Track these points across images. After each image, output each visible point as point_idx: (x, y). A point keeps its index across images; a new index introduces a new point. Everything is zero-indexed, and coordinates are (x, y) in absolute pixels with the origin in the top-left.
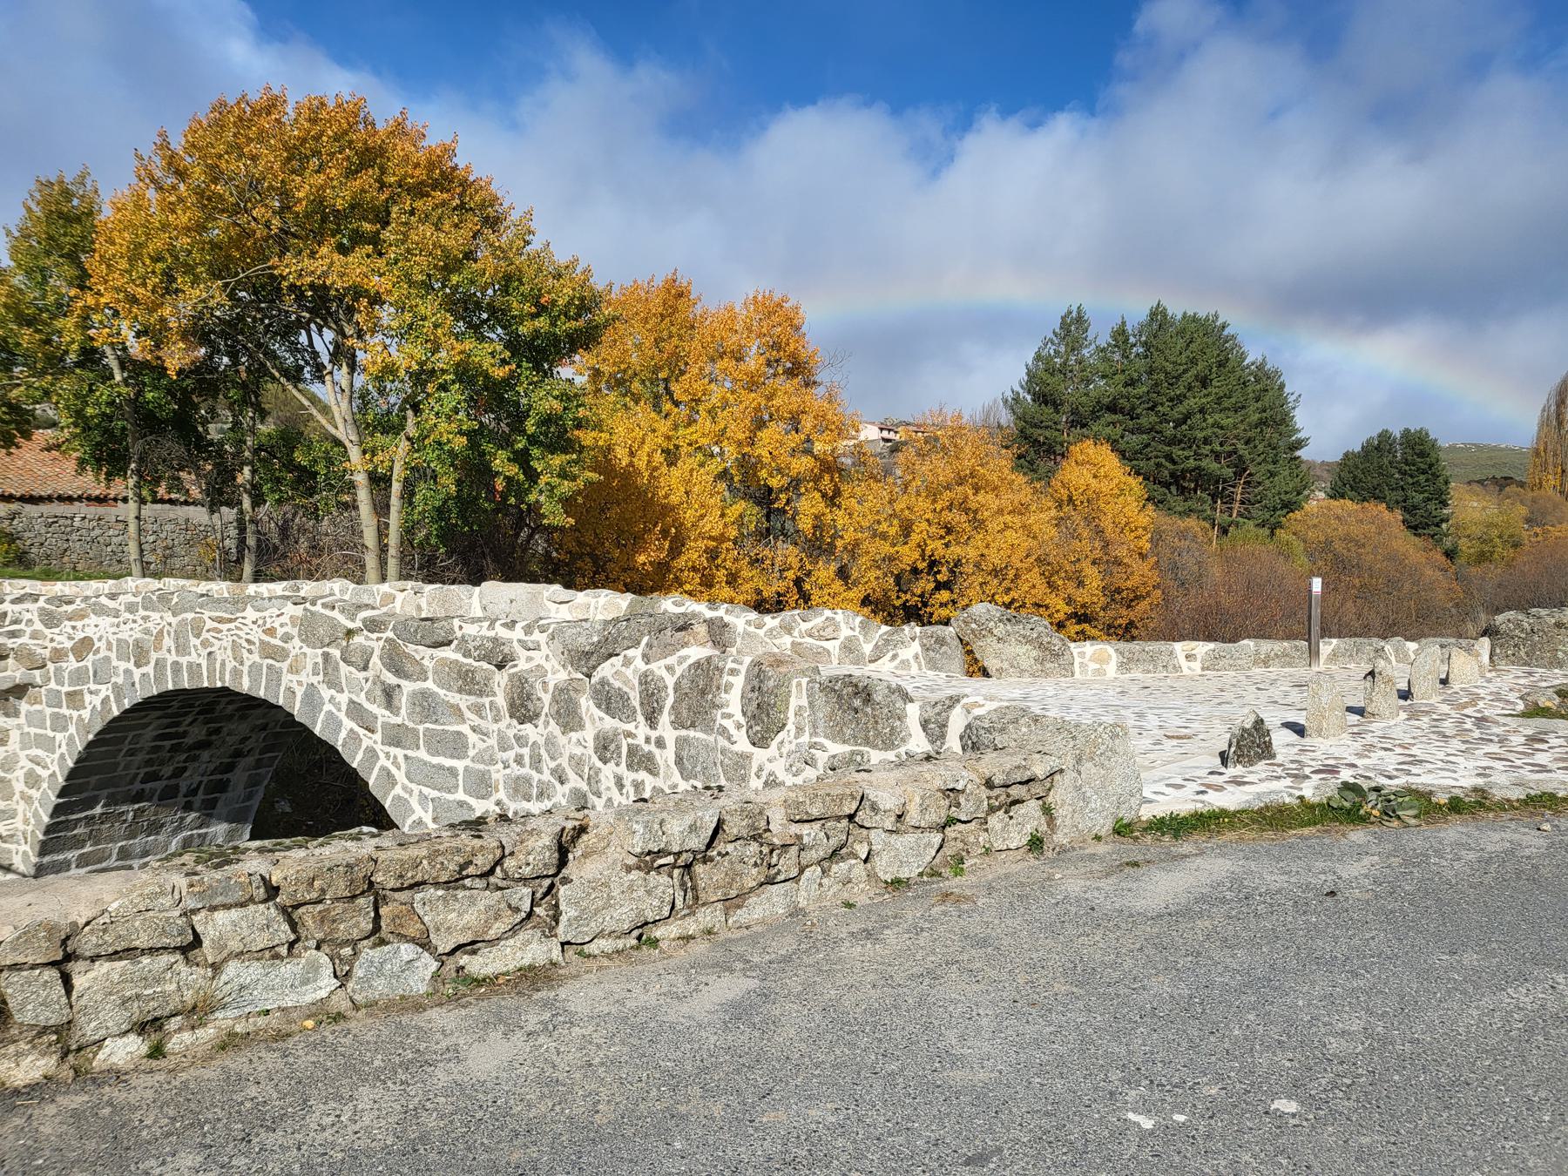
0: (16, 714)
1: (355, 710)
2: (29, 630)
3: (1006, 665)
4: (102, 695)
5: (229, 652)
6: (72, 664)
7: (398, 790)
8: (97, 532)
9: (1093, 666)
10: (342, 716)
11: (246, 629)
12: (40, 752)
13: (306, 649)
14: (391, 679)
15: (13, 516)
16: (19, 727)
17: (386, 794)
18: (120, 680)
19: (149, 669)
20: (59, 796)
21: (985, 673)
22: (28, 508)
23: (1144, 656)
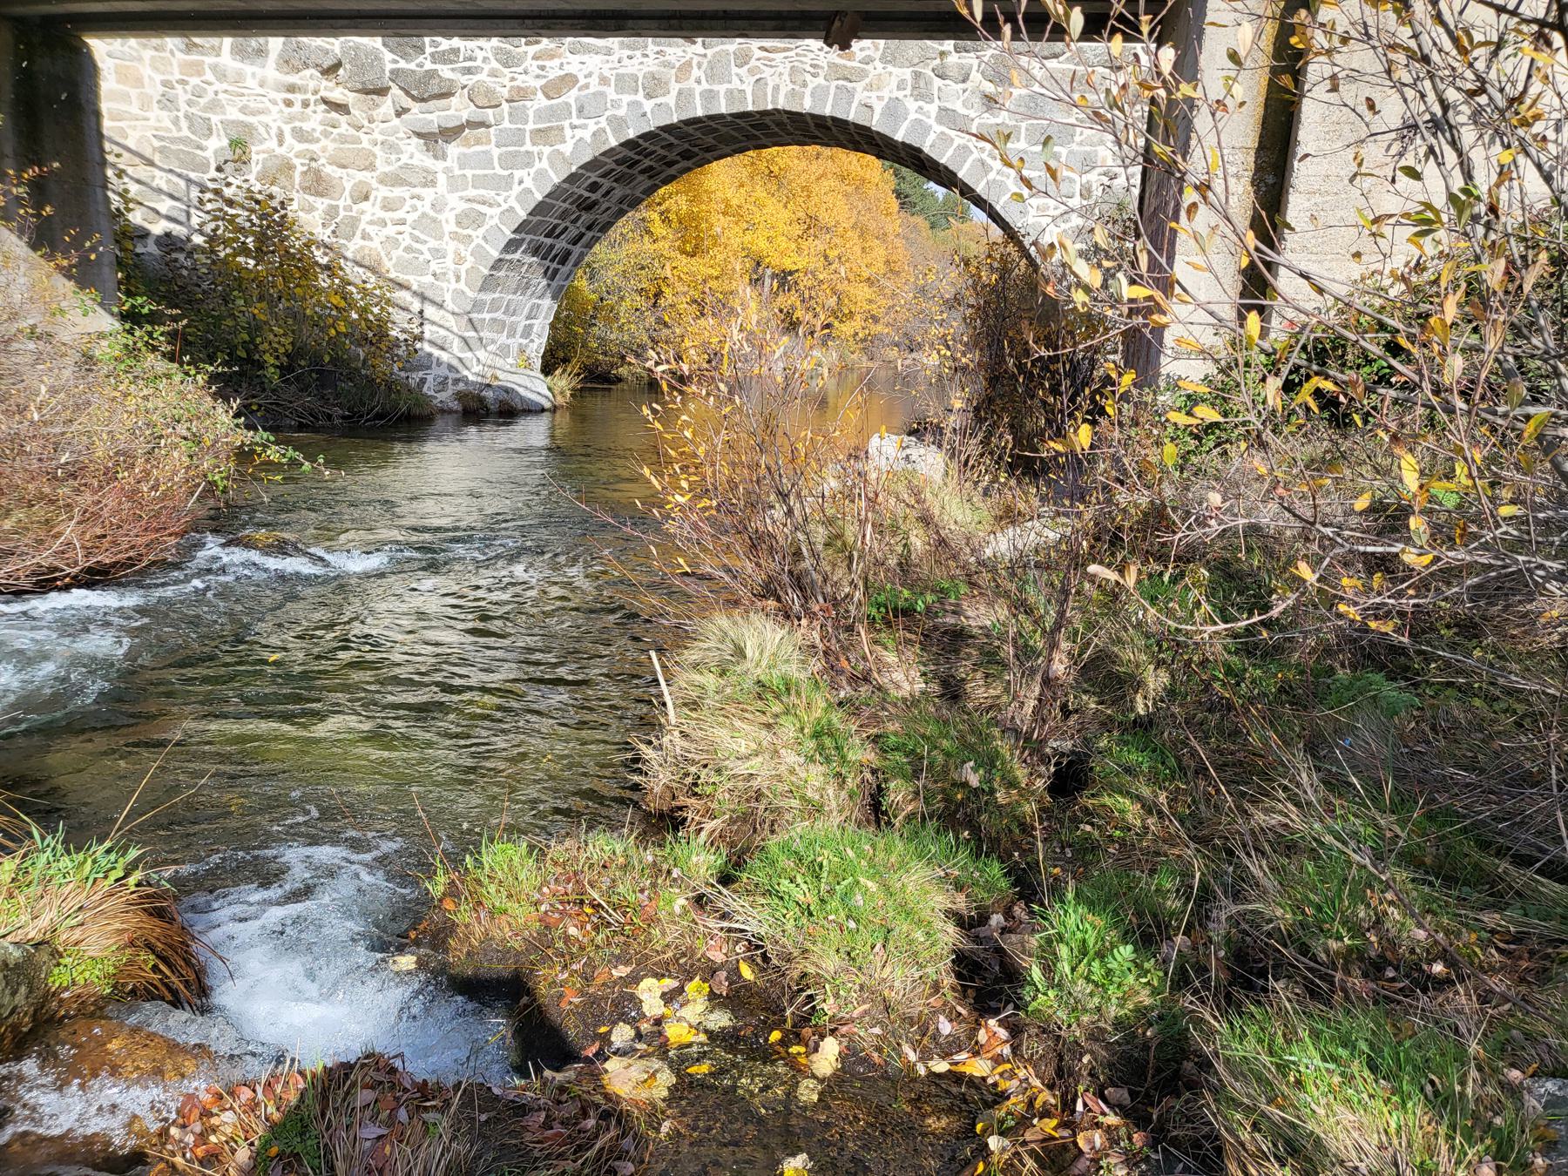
0: (444, 157)
1: (946, 115)
2: (487, 68)
4: (592, 126)
5: (786, 77)
6: (541, 101)
7: (991, 176)
10: (931, 122)
11: (811, 55)
12: (482, 192)
13: (890, 68)
14: (989, 88)
16: (447, 170)
17: (978, 181)
18: (622, 112)
19: (671, 100)
20: (515, 232)
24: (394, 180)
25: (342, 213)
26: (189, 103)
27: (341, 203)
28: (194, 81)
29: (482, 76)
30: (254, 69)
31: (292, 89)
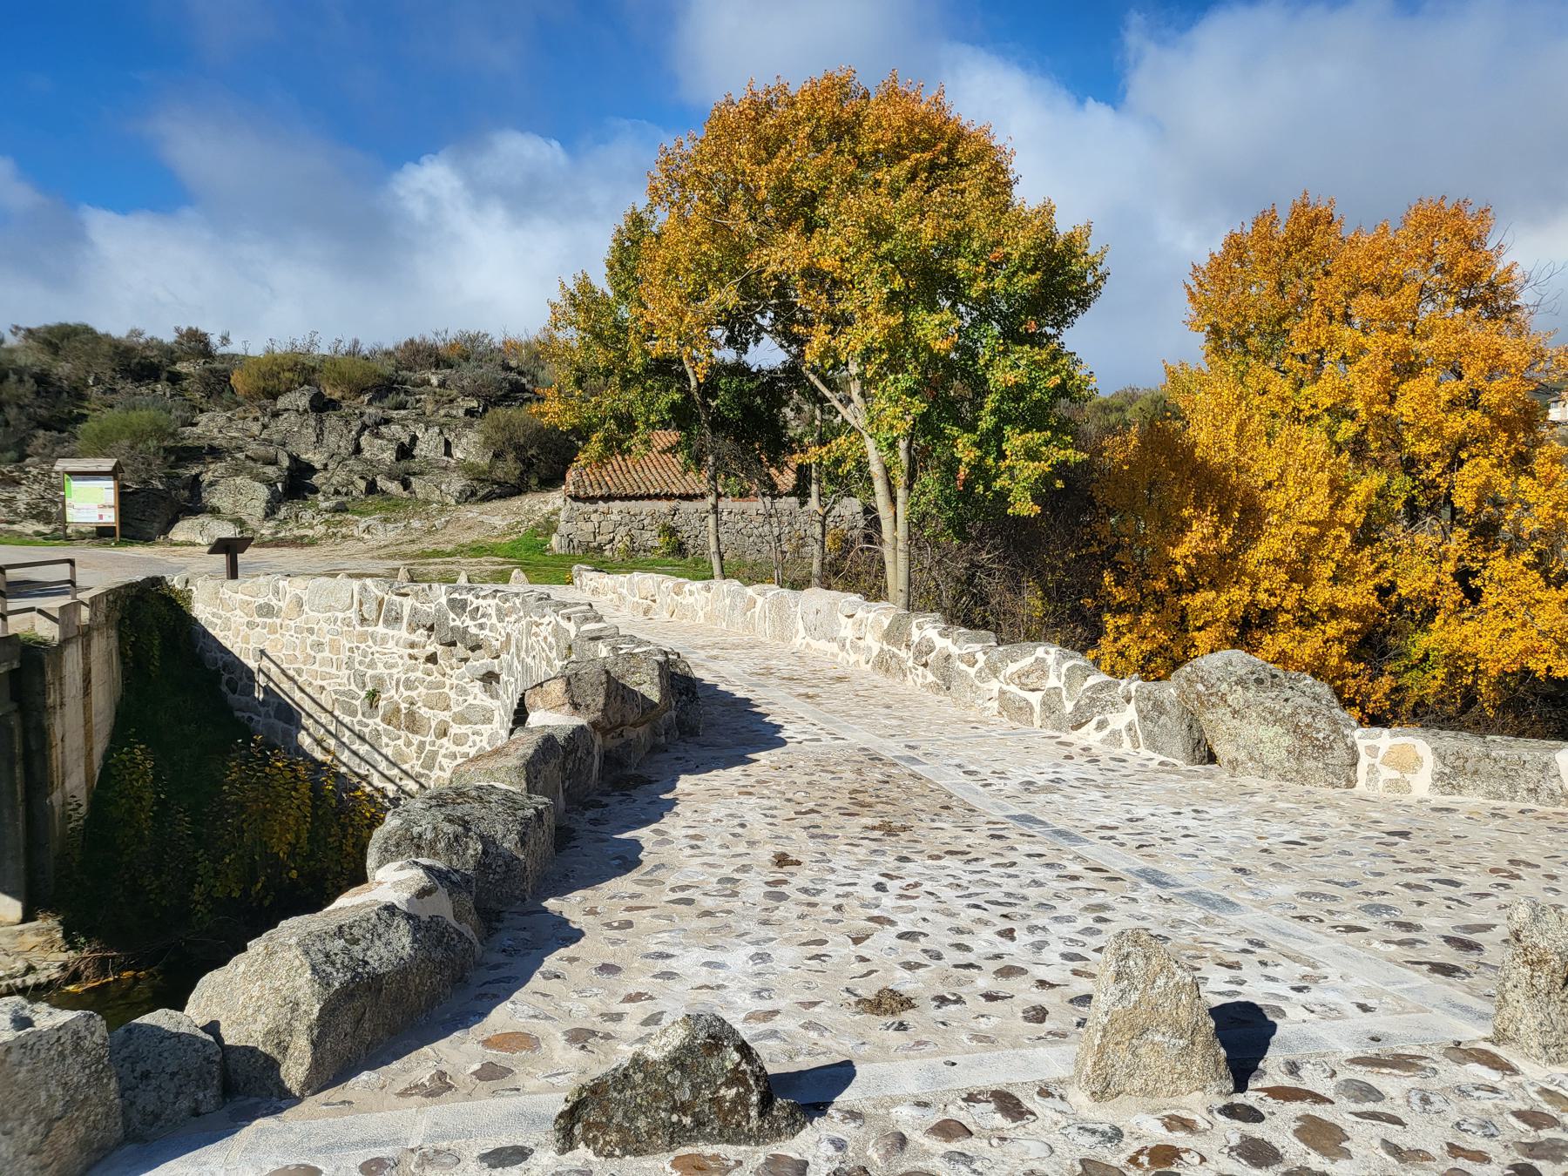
3: (1242, 756)
8: (742, 524)
9: (1387, 773)
15: (675, 511)
21: (1212, 758)
22: (685, 505)
23: (1486, 766)
24: (462, 719)
25: (428, 747)
26: (360, 663)
27: (428, 739)
28: (363, 646)
29: (487, 632)
30: (395, 632)
31: (412, 645)
